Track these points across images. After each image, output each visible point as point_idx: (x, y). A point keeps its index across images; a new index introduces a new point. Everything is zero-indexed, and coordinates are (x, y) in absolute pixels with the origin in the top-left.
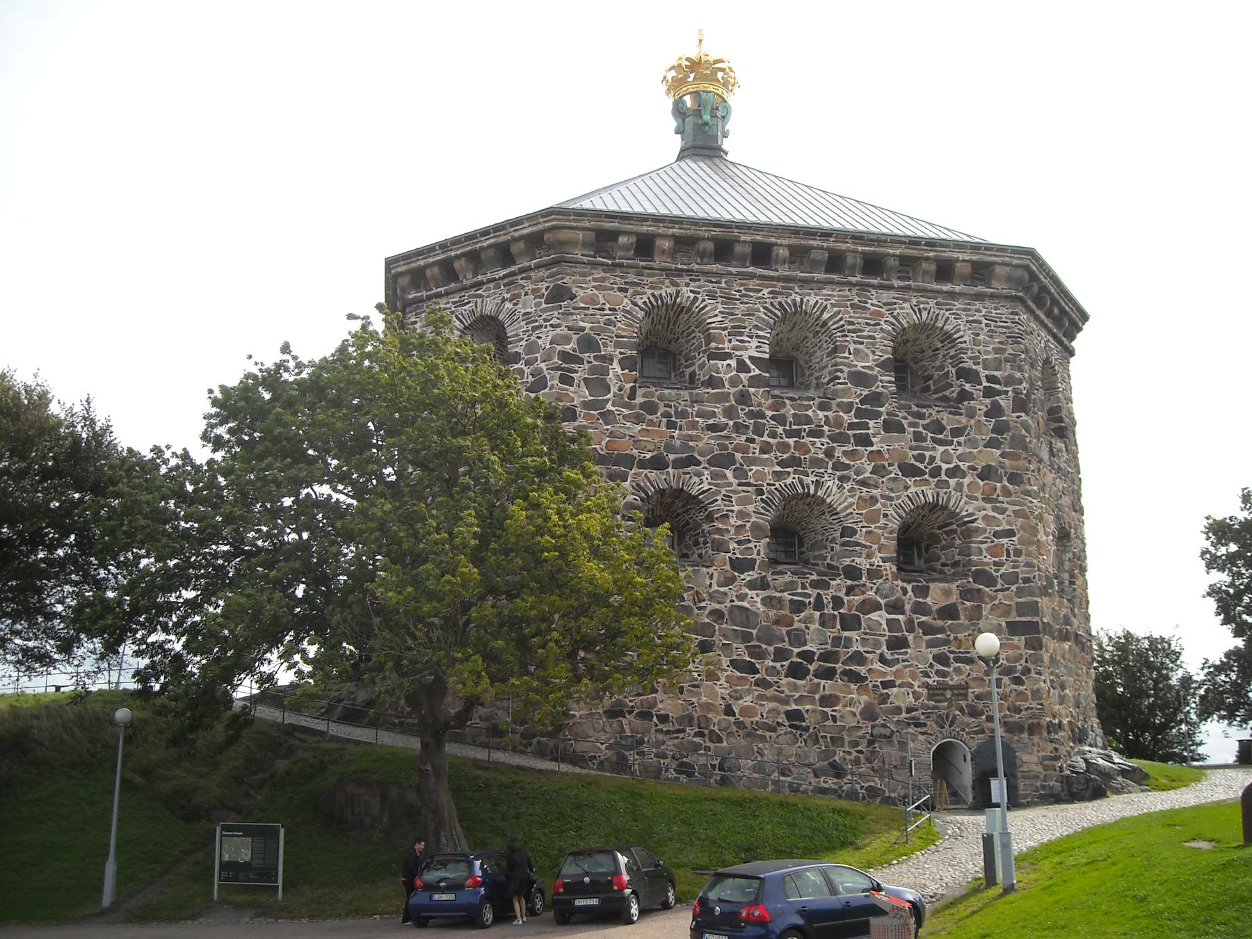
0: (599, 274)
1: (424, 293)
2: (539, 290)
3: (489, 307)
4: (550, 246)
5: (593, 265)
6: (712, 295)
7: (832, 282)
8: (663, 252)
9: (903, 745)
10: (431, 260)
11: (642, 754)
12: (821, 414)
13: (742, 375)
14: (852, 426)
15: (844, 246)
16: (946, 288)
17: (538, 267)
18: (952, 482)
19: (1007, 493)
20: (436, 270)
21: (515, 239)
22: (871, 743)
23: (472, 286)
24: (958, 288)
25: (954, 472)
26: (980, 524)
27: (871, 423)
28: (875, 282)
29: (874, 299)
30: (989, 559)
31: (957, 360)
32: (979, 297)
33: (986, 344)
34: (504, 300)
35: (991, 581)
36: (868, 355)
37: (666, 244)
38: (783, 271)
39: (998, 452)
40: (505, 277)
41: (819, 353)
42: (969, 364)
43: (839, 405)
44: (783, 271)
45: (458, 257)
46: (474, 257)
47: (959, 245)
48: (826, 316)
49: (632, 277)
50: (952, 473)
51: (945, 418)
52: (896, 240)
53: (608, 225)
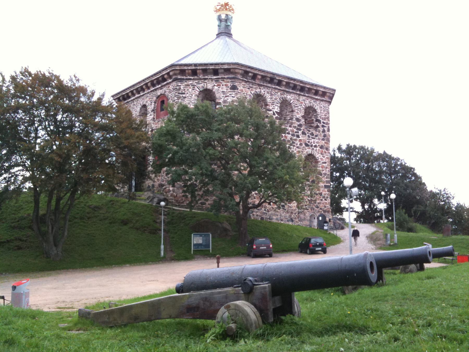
0: (244, 83)
1: (185, 77)
2: (227, 85)
3: (210, 86)
4: (232, 73)
5: (243, 80)
6: (268, 93)
7: (293, 93)
8: (258, 79)
9: (305, 214)
10: (189, 68)
11: (253, 215)
12: (290, 128)
13: (274, 116)
14: (296, 132)
15: (298, 84)
16: (316, 97)
17: (228, 78)
18: (315, 149)
19: (325, 153)
20: (190, 71)
21: (221, 69)
22: (298, 213)
23: (203, 79)
24: (319, 98)
25: (315, 146)
26: (320, 160)
27: (300, 132)
28: (302, 94)
29: (302, 98)
30: (321, 169)
31: (316, 116)
32: (322, 101)
33: (323, 113)
34: (214, 85)
35: (321, 175)
36: (299, 113)
37: (260, 77)
38: (283, 88)
39: (324, 142)
40: (216, 79)
41: (285, 111)
42: (319, 118)
43: (294, 126)
44: (283, 88)
45: (199, 69)
46: (205, 71)
47: (321, 87)
48: (291, 102)
49: (251, 85)
50: (315, 146)
51: (314, 132)
52: (309, 84)
53: (248, 70)
